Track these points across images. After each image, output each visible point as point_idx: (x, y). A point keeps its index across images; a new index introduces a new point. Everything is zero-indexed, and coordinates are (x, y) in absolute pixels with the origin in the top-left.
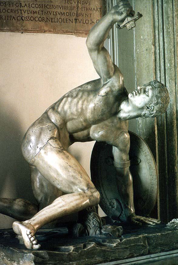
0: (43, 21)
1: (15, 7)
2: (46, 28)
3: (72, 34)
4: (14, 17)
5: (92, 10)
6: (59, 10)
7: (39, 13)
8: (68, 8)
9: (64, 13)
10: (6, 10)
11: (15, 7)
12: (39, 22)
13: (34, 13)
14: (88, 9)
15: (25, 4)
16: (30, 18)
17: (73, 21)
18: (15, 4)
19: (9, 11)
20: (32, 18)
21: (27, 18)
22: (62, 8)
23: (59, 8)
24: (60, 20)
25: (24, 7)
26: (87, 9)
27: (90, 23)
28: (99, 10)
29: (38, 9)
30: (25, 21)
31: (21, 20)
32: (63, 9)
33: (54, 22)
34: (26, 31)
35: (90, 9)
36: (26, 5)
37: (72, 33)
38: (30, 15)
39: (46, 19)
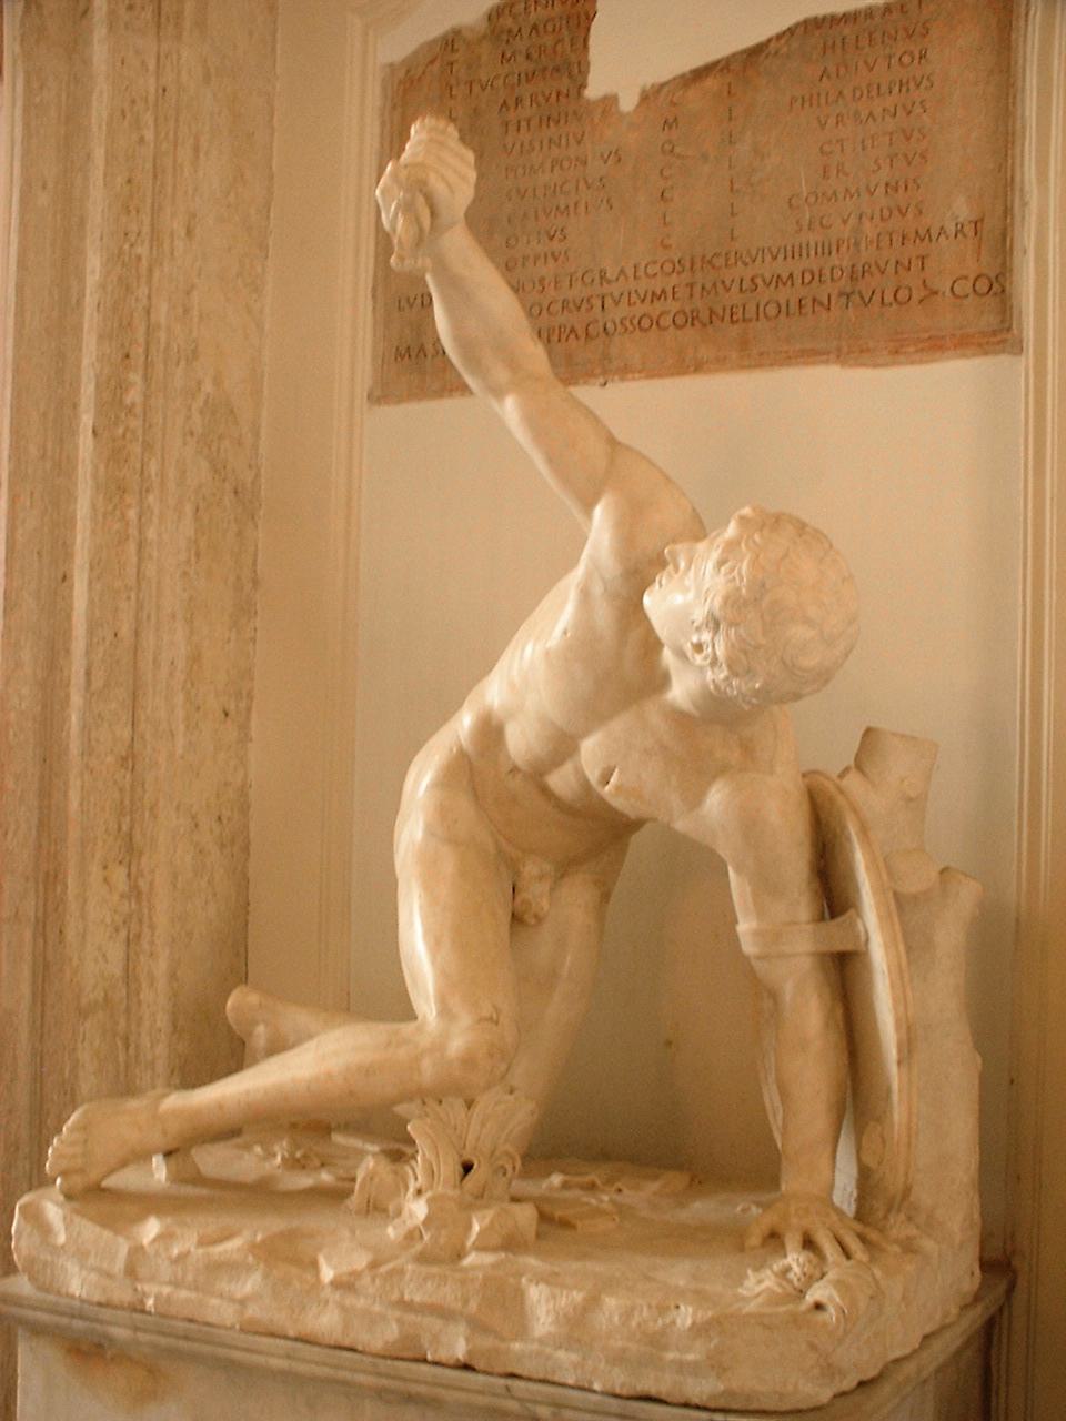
0: (693, 325)
1: (578, 285)
2: (705, 352)
3: (827, 362)
4: (572, 330)
5: (934, 239)
6: (767, 269)
7: (674, 293)
8: (812, 253)
9: (791, 275)
10: (545, 305)
11: (578, 285)
12: (679, 332)
13: (655, 297)
14: (912, 236)
15: (619, 269)
16: (636, 322)
17: (833, 302)
18: (580, 275)
19: (557, 307)
20: (646, 323)
21: (628, 323)
22: (781, 257)
23: (768, 258)
24: (772, 310)
25: (617, 279)
26: (903, 238)
27: (916, 297)
28: (969, 230)
29: (674, 279)
30: (616, 338)
31: (604, 335)
32: (785, 258)
33: (744, 320)
34: (625, 372)
35: (922, 233)
36: (622, 271)
37: (825, 357)
38: (639, 309)
39: (704, 316)
